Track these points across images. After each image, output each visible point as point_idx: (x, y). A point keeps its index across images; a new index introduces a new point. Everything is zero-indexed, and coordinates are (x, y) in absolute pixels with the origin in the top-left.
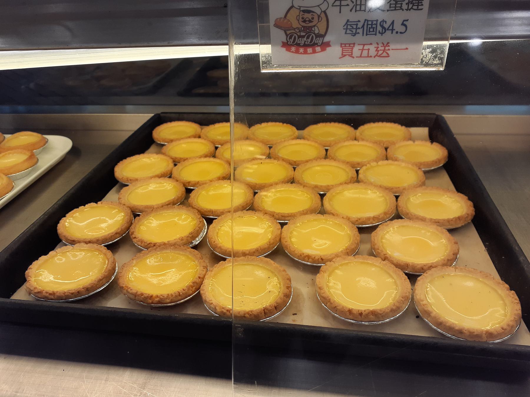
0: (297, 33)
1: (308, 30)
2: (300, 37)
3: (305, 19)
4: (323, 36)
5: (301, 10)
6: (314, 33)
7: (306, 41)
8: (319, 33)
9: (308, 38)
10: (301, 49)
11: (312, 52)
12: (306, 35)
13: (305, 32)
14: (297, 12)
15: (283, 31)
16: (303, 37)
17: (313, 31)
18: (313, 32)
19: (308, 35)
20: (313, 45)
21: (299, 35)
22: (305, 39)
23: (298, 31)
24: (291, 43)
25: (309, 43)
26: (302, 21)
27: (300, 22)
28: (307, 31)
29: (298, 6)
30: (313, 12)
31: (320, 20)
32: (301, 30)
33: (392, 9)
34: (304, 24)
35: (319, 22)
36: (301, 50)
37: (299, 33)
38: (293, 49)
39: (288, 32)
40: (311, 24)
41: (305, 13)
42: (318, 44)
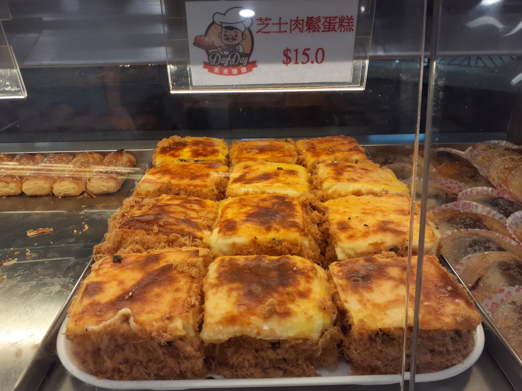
0: (220, 52)
2: (223, 56)
4: (249, 56)
6: (239, 52)
7: (230, 60)
8: (244, 52)
9: (232, 57)
14: (219, 29)
16: (227, 56)
17: (237, 49)
18: (237, 51)
19: (231, 54)
22: (229, 59)
23: (221, 50)
27: (222, 40)
29: (220, 22)
30: (236, 29)
31: (244, 39)
33: (326, 30)
35: (243, 40)
36: (226, 71)
38: (217, 70)
39: (210, 51)
40: (235, 42)
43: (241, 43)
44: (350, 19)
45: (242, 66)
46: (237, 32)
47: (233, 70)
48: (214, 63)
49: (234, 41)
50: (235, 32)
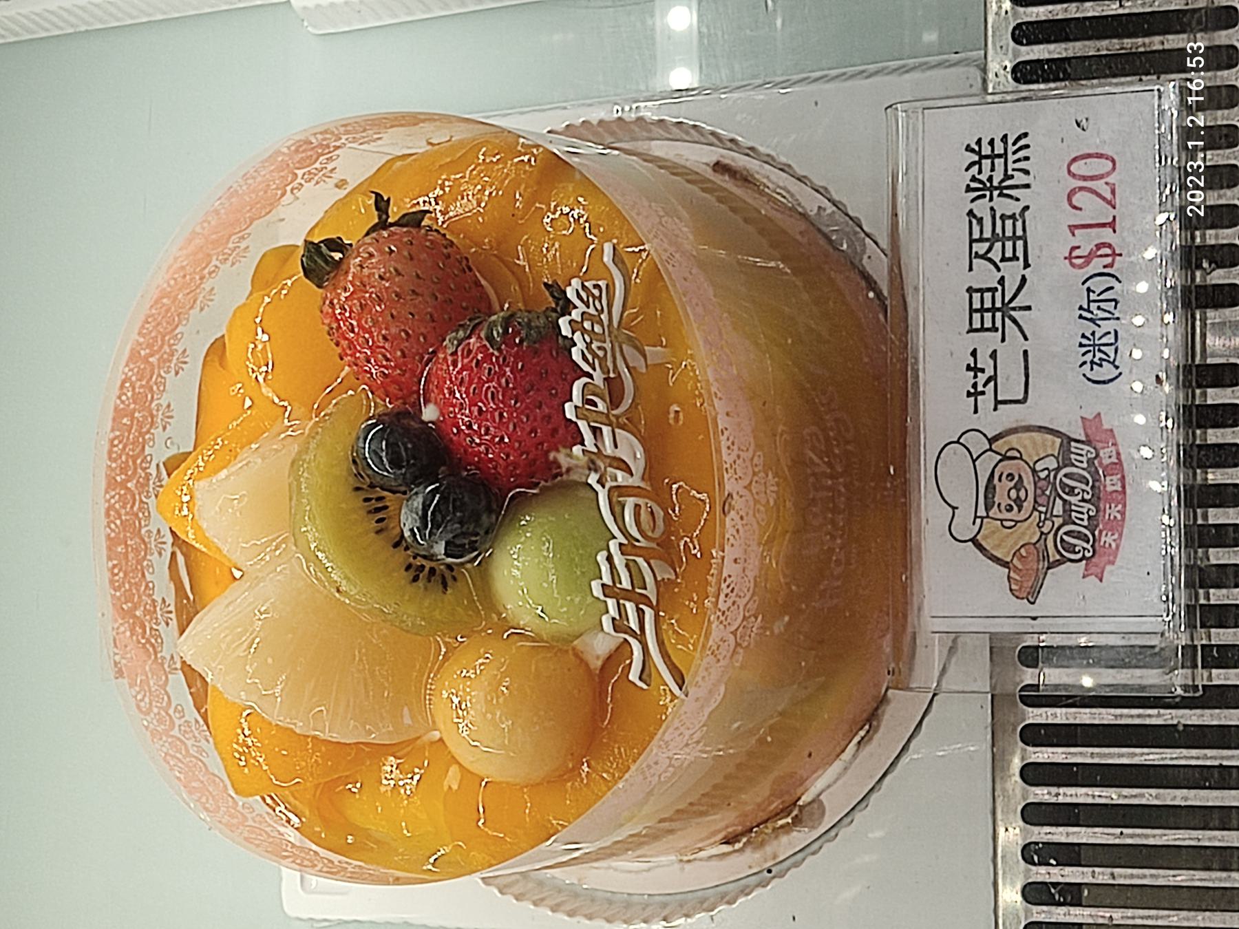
0: (1056, 526)
1: (1048, 493)
5: (985, 514)
6: (1058, 469)
7: (1080, 497)
8: (1056, 454)
10: (1108, 511)
11: (1119, 476)
12: (1061, 498)
13: (1052, 499)
15: (1050, 571)
17: (1048, 476)
18: (1052, 474)
22: (1073, 500)
23: (1049, 523)
24: (1089, 547)
25: (1088, 489)
26: (1020, 511)
29: (974, 523)
31: (1018, 455)
34: (1028, 505)
35: (1021, 458)
36: (1113, 511)
38: (1107, 539)
41: (994, 502)
43: (1032, 465)
44: (979, 153)
45: (1096, 462)
48: (1089, 547)
49: (1025, 483)
50: (1000, 480)
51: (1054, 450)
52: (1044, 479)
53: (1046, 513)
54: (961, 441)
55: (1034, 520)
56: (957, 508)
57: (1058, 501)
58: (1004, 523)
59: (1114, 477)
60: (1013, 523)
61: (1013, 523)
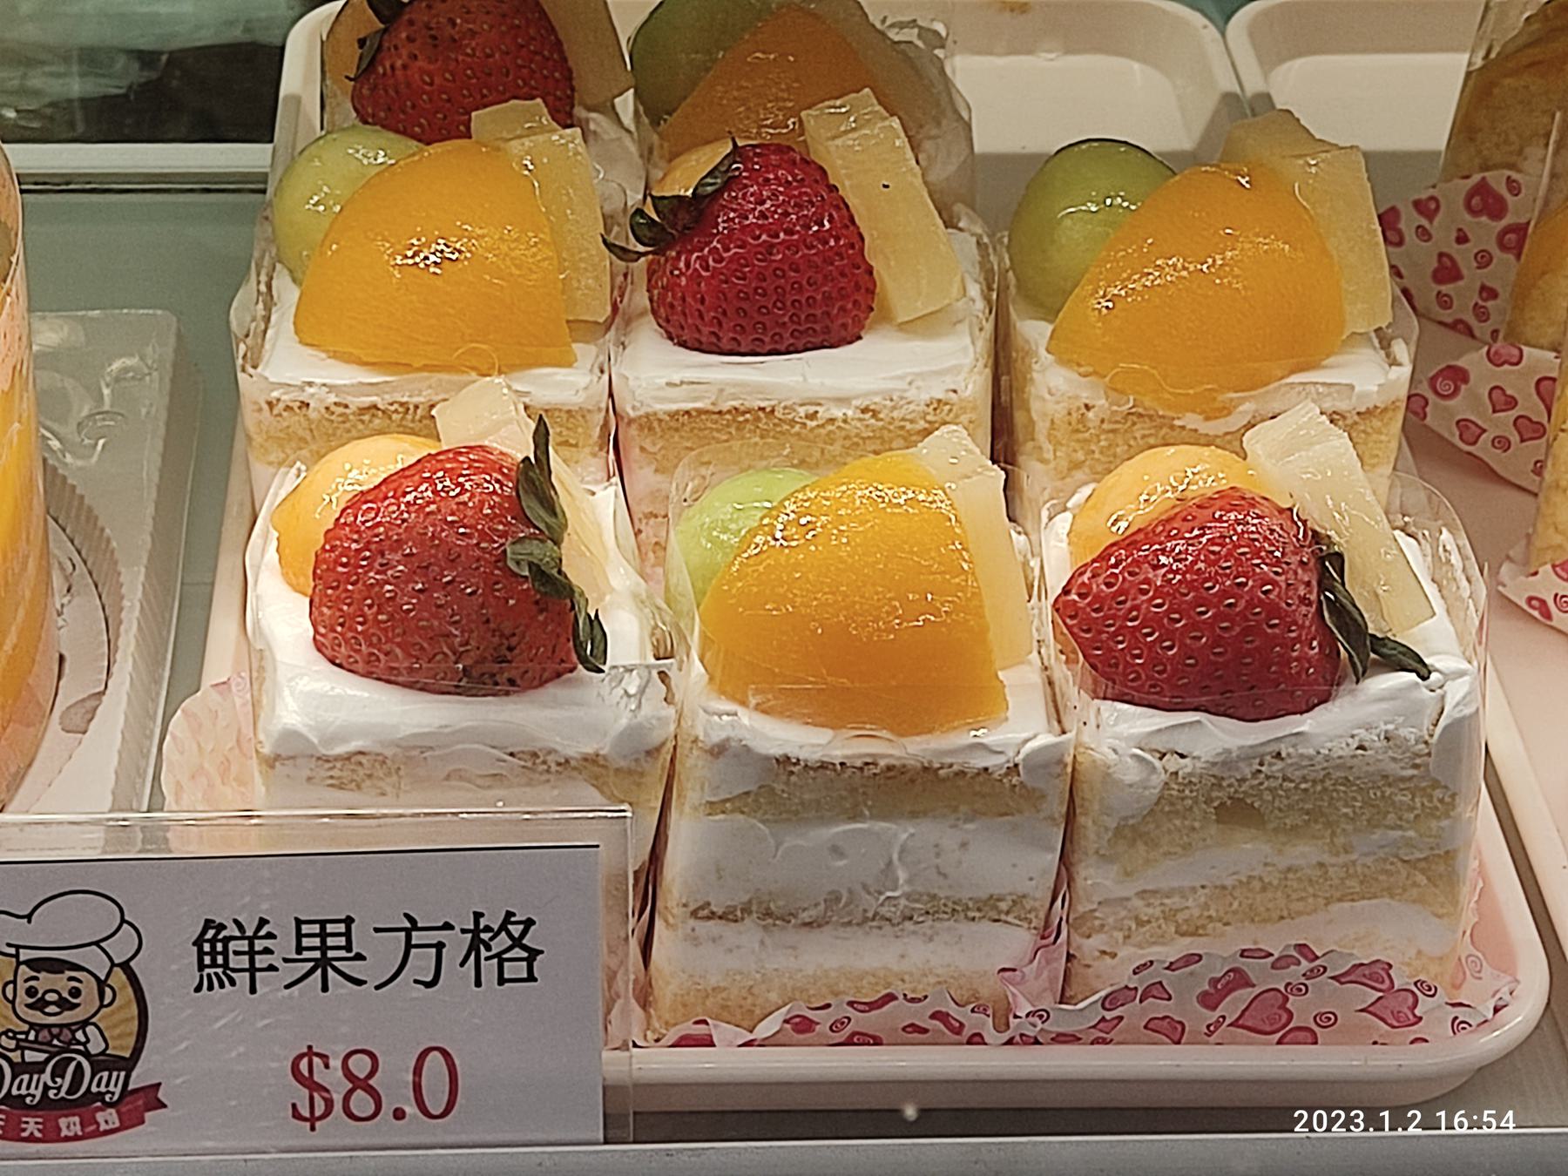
0: (10, 1055)
1: (55, 1042)
2: (18, 1069)
3: (39, 995)
4: (128, 1064)
5: (22, 958)
6: (86, 1054)
7: (50, 1084)
9: (58, 1072)
11: (80, 1133)
12: (47, 1061)
13: (44, 1047)
16: (39, 1068)
17: (79, 1043)
18: (81, 1048)
20: (84, 1104)
21: (19, 1060)
22: (46, 1077)
23: (12, 1044)
25: (62, 1094)
26: (28, 1006)
28: (56, 1046)
29: (9, 945)
31: (106, 1002)
32: (26, 1040)
34: (37, 1016)
35: (102, 1006)
36: (32, 1125)
37: (19, 1052)
40: (68, 1017)
41: (39, 972)
42: (107, 1098)
43: (93, 1020)
45: (99, 1104)
46: (80, 981)
47: (63, 1122)
49: (66, 1013)
50: (71, 979)
51: (114, 1048)
52: (74, 1038)
53: (26, 1040)
54: (125, 926)
55: (17, 1026)
56: (29, 922)
57: (42, 1057)
58: (11, 986)
59: (78, 1127)
60: (10, 997)
61: (10, 997)
